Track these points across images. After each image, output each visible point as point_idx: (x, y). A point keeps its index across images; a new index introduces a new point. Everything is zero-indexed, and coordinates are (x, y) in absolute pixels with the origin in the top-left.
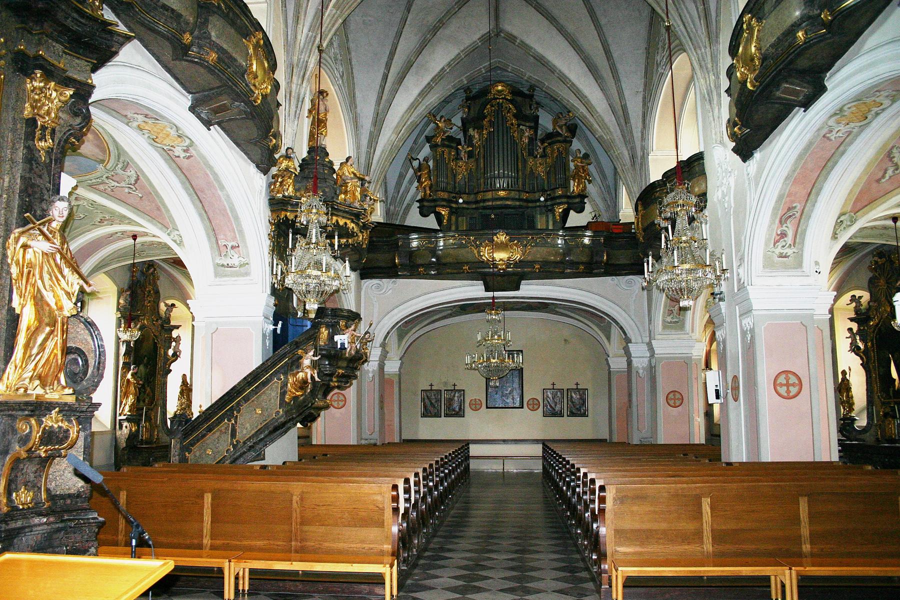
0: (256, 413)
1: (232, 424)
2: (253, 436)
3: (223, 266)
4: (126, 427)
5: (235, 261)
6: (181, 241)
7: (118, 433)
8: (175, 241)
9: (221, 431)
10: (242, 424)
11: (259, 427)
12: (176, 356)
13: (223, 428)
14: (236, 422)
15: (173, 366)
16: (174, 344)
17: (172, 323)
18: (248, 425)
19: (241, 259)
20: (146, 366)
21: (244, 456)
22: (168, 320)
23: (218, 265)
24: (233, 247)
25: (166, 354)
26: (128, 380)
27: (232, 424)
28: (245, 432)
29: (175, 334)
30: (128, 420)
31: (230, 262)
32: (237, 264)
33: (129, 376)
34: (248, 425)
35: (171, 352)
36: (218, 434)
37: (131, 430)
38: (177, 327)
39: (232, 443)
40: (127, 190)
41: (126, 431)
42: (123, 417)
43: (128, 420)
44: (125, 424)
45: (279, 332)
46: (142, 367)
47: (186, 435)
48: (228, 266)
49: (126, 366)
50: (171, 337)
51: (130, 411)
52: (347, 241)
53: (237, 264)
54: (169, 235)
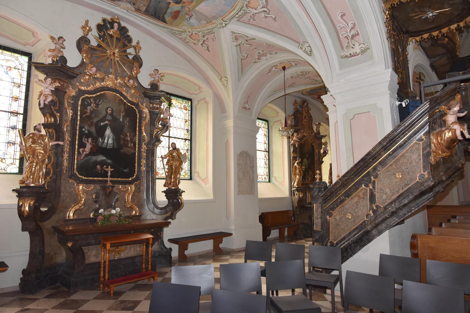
0: (396, 178)
1: (370, 189)
2: (394, 201)
3: (346, 57)
4: (297, 195)
5: (357, 49)
6: (311, 51)
7: (293, 198)
8: (307, 53)
9: (359, 196)
10: (381, 189)
11: (401, 192)
12: (325, 153)
13: (361, 193)
14: (374, 187)
15: (324, 159)
16: (323, 146)
17: (321, 134)
18: (387, 190)
19: (362, 45)
20: (308, 159)
21: (386, 222)
22: (319, 133)
23: (342, 57)
24: (353, 37)
25: (319, 152)
26: (296, 166)
27: (370, 189)
28: (384, 197)
29: (323, 141)
30: (297, 190)
31: (352, 51)
32: (358, 51)
33: (296, 164)
34: (387, 190)
35: (322, 151)
36: (356, 199)
37: (299, 196)
38: (324, 136)
39: (371, 208)
40: (263, 15)
41: (296, 197)
42: (294, 189)
43: (297, 190)
44: (296, 193)
45: (404, 105)
46: (305, 160)
47: (325, 200)
48: (351, 56)
49: (295, 158)
50: (321, 142)
51: (297, 185)
52: (458, 25)
53: (358, 51)
54: (301, 48)
